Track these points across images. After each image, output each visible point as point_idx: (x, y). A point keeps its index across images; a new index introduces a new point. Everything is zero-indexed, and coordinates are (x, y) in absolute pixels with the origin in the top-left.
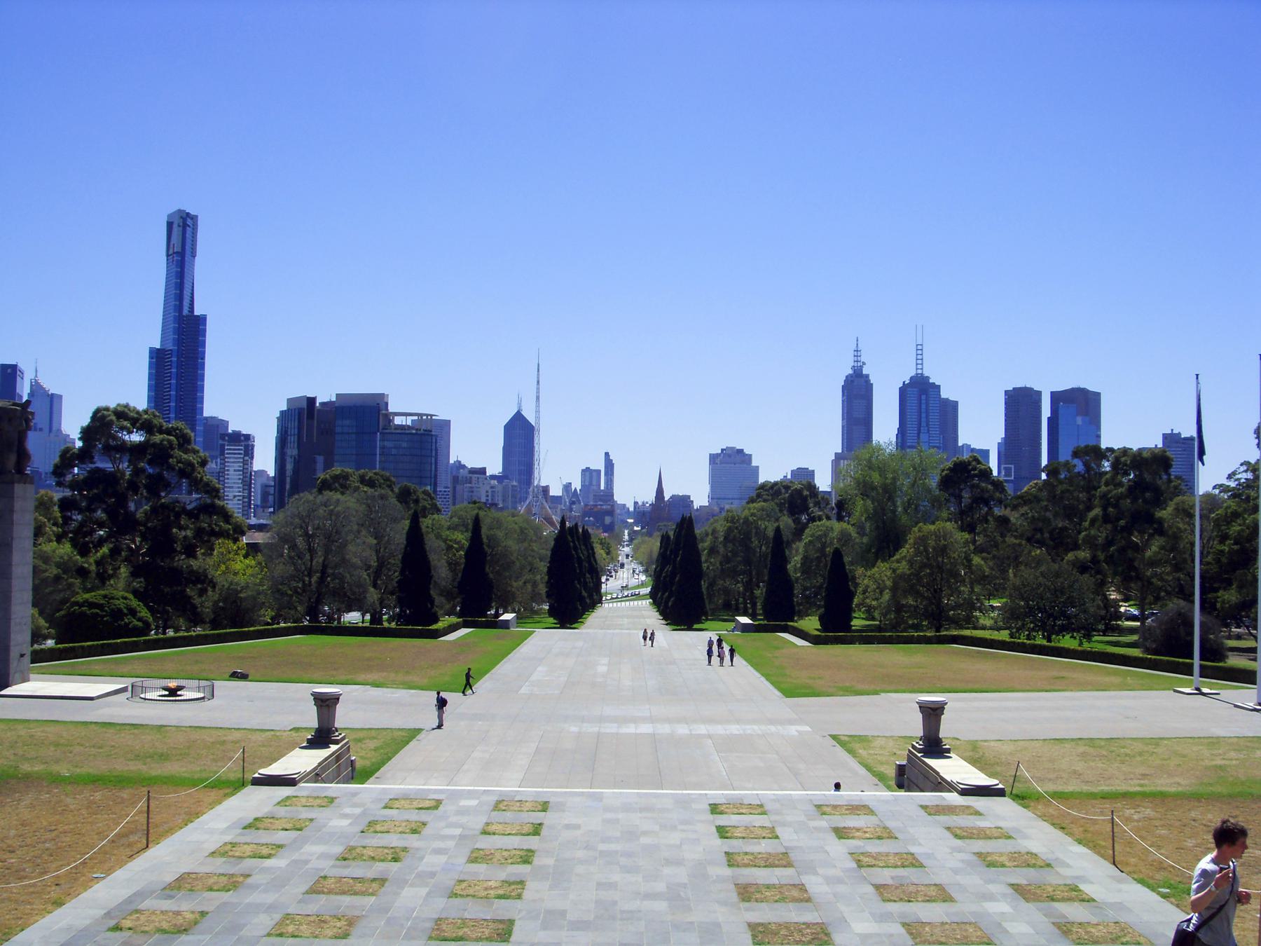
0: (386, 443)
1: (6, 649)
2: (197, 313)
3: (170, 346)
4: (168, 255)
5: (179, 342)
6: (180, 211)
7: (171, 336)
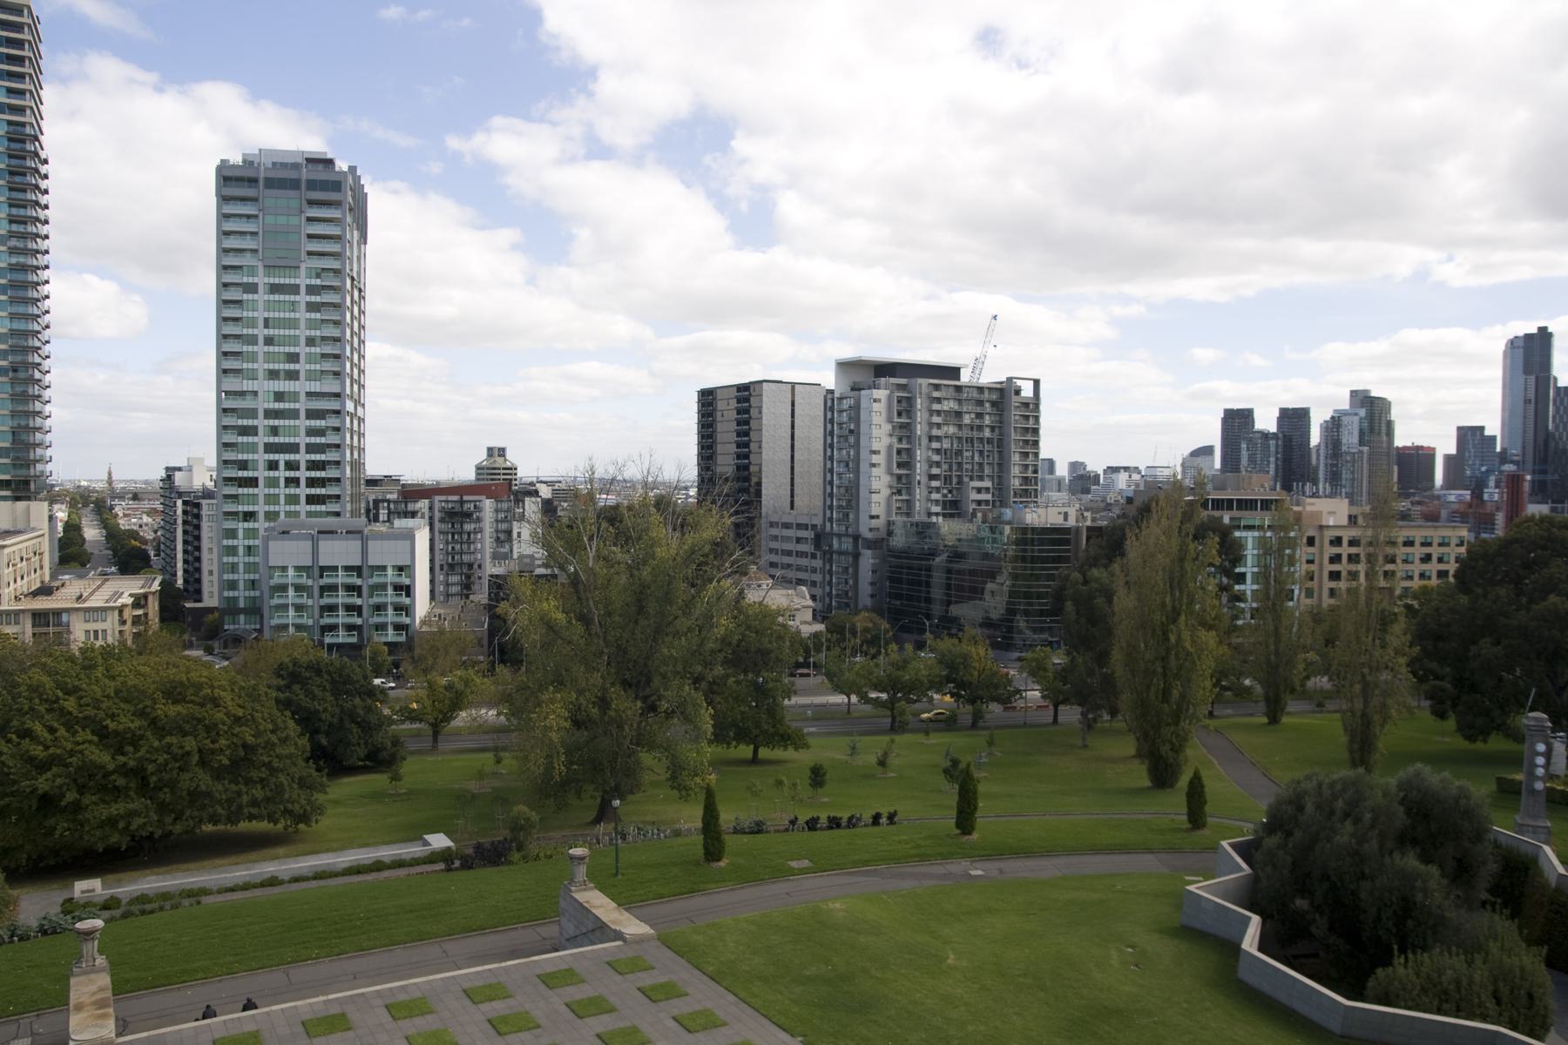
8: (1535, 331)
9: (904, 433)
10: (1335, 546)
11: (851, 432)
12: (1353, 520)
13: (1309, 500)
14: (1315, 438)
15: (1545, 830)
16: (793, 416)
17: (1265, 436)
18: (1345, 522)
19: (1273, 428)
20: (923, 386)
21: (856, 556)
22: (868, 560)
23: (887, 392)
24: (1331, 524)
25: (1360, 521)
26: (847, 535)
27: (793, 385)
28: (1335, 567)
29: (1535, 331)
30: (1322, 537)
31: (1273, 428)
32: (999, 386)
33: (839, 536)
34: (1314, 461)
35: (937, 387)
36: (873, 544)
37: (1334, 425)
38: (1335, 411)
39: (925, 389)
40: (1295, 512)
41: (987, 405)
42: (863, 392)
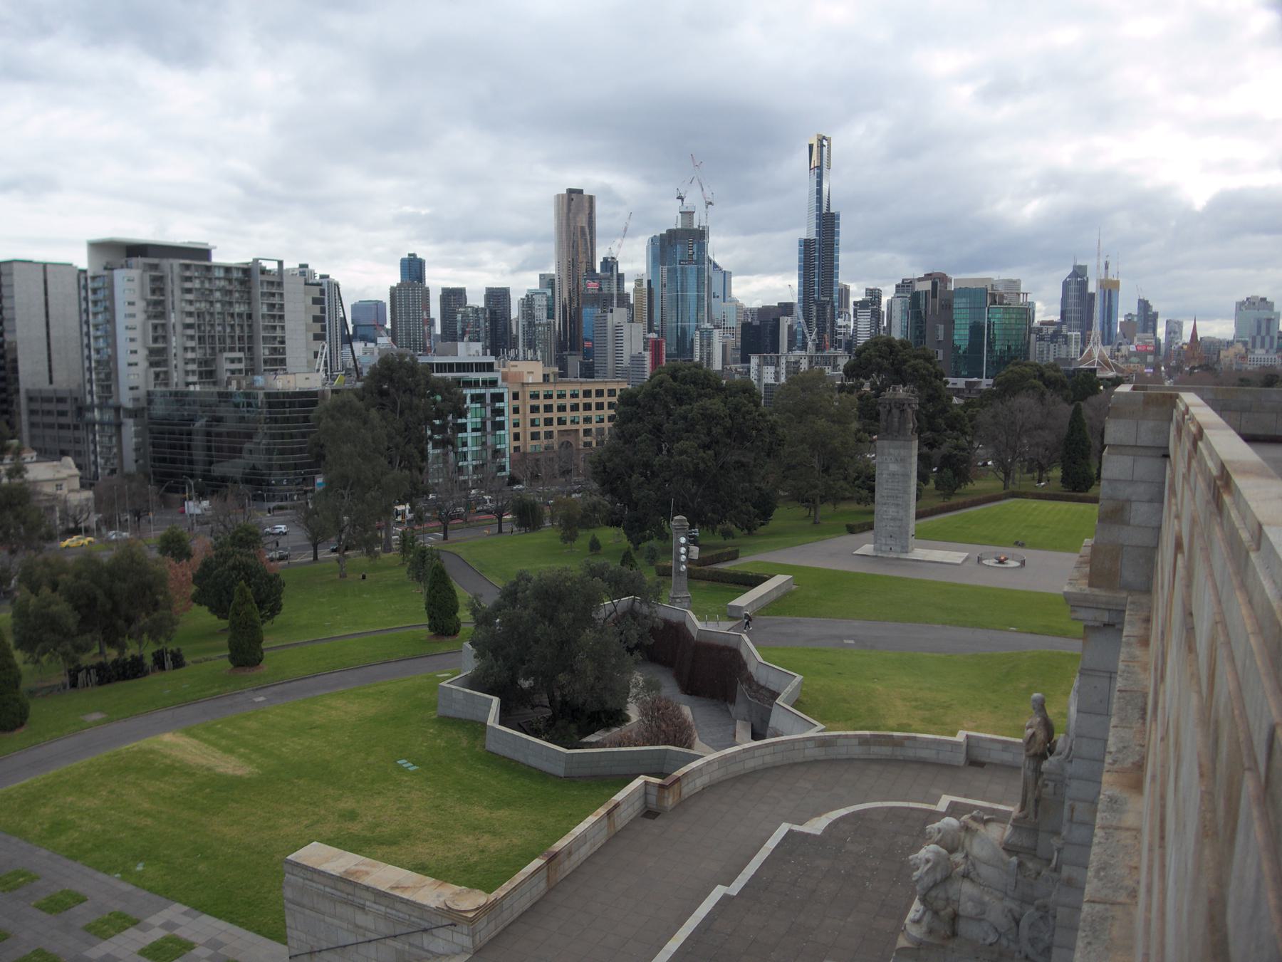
1: (907, 532)
2: (831, 211)
3: (813, 236)
12: (546, 377)
14: (515, 313)
15: (688, 600)
16: (46, 294)
18: (541, 380)
19: (482, 304)
20: (175, 266)
21: (119, 426)
22: (130, 428)
25: (552, 380)
27: (45, 265)
30: (524, 392)
31: (482, 304)
34: (514, 331)
36: (135, 413)
37: (528, 302)
38: (529, 290)
39: (177, 270)
40: (502, 373)
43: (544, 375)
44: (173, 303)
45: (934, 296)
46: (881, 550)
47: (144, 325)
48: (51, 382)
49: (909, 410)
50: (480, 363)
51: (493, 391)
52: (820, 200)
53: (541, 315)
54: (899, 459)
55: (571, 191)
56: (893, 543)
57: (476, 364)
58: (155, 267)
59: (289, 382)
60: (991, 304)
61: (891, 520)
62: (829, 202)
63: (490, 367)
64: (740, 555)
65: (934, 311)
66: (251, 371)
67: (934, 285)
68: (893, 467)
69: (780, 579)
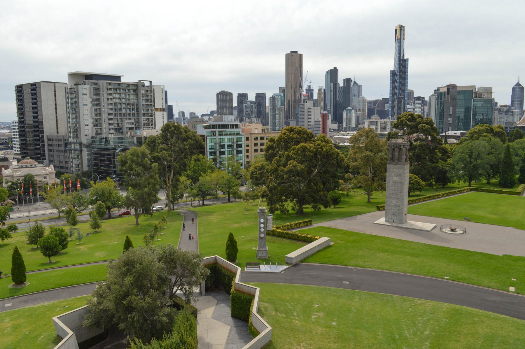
0: (475, 103)
2: (405, 58)
4: (396, 40)
5: (400, 68)
6: (399, 25)
7: (397, 66)
8: (333, 69)
9: (97, 102)
10: (256, 140)
11: (76, 102)
13: (247, 124)
14: (267, 104)
15: (266, 252)
16: (55, 96)
17: (252, 102)
18: (261, 132)
20: (104, 84)
21: (81, 151)
22: (85, 152)
23: (89, 86)
24: (256, 132)
26: (77, 143)
27: (55, 83)
28: (256, 148)
29: (333, 69)
30: (251, 137)
32: (136, 84)
33: (74, 143)
35: (110, 84)
36: (88, 146)
37: (273, 99)
38: (274, 94)
39: (105, 85)
41: (132, 91)
42: (79, 86)
43: (262, 130)
44: (103, 99)
45: (448, 93)
46: (389, 222)
47: (91, 108)
48: (58, 133)
49: (404, 149)
50: (215, 125)
51: (237, 137)
52: (400, 54)
53: (278, 103)
54: (398, 174)
55: (292, 52)
56: (395, 218)
57: (230, 125)
58: (96, 84)
59: (149, 133)
60: (475, 97)
61: (394, 205)
62: (404, 53)
63: (237, 126)
64: (312, 223)
65: (448, 101)
66: (138, 128)
67: (448, 89)
68: (395, 179)
69: (324, 239)
